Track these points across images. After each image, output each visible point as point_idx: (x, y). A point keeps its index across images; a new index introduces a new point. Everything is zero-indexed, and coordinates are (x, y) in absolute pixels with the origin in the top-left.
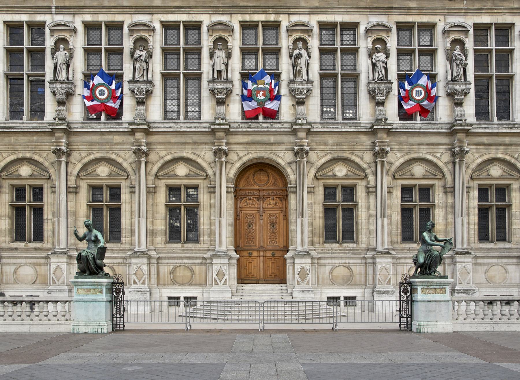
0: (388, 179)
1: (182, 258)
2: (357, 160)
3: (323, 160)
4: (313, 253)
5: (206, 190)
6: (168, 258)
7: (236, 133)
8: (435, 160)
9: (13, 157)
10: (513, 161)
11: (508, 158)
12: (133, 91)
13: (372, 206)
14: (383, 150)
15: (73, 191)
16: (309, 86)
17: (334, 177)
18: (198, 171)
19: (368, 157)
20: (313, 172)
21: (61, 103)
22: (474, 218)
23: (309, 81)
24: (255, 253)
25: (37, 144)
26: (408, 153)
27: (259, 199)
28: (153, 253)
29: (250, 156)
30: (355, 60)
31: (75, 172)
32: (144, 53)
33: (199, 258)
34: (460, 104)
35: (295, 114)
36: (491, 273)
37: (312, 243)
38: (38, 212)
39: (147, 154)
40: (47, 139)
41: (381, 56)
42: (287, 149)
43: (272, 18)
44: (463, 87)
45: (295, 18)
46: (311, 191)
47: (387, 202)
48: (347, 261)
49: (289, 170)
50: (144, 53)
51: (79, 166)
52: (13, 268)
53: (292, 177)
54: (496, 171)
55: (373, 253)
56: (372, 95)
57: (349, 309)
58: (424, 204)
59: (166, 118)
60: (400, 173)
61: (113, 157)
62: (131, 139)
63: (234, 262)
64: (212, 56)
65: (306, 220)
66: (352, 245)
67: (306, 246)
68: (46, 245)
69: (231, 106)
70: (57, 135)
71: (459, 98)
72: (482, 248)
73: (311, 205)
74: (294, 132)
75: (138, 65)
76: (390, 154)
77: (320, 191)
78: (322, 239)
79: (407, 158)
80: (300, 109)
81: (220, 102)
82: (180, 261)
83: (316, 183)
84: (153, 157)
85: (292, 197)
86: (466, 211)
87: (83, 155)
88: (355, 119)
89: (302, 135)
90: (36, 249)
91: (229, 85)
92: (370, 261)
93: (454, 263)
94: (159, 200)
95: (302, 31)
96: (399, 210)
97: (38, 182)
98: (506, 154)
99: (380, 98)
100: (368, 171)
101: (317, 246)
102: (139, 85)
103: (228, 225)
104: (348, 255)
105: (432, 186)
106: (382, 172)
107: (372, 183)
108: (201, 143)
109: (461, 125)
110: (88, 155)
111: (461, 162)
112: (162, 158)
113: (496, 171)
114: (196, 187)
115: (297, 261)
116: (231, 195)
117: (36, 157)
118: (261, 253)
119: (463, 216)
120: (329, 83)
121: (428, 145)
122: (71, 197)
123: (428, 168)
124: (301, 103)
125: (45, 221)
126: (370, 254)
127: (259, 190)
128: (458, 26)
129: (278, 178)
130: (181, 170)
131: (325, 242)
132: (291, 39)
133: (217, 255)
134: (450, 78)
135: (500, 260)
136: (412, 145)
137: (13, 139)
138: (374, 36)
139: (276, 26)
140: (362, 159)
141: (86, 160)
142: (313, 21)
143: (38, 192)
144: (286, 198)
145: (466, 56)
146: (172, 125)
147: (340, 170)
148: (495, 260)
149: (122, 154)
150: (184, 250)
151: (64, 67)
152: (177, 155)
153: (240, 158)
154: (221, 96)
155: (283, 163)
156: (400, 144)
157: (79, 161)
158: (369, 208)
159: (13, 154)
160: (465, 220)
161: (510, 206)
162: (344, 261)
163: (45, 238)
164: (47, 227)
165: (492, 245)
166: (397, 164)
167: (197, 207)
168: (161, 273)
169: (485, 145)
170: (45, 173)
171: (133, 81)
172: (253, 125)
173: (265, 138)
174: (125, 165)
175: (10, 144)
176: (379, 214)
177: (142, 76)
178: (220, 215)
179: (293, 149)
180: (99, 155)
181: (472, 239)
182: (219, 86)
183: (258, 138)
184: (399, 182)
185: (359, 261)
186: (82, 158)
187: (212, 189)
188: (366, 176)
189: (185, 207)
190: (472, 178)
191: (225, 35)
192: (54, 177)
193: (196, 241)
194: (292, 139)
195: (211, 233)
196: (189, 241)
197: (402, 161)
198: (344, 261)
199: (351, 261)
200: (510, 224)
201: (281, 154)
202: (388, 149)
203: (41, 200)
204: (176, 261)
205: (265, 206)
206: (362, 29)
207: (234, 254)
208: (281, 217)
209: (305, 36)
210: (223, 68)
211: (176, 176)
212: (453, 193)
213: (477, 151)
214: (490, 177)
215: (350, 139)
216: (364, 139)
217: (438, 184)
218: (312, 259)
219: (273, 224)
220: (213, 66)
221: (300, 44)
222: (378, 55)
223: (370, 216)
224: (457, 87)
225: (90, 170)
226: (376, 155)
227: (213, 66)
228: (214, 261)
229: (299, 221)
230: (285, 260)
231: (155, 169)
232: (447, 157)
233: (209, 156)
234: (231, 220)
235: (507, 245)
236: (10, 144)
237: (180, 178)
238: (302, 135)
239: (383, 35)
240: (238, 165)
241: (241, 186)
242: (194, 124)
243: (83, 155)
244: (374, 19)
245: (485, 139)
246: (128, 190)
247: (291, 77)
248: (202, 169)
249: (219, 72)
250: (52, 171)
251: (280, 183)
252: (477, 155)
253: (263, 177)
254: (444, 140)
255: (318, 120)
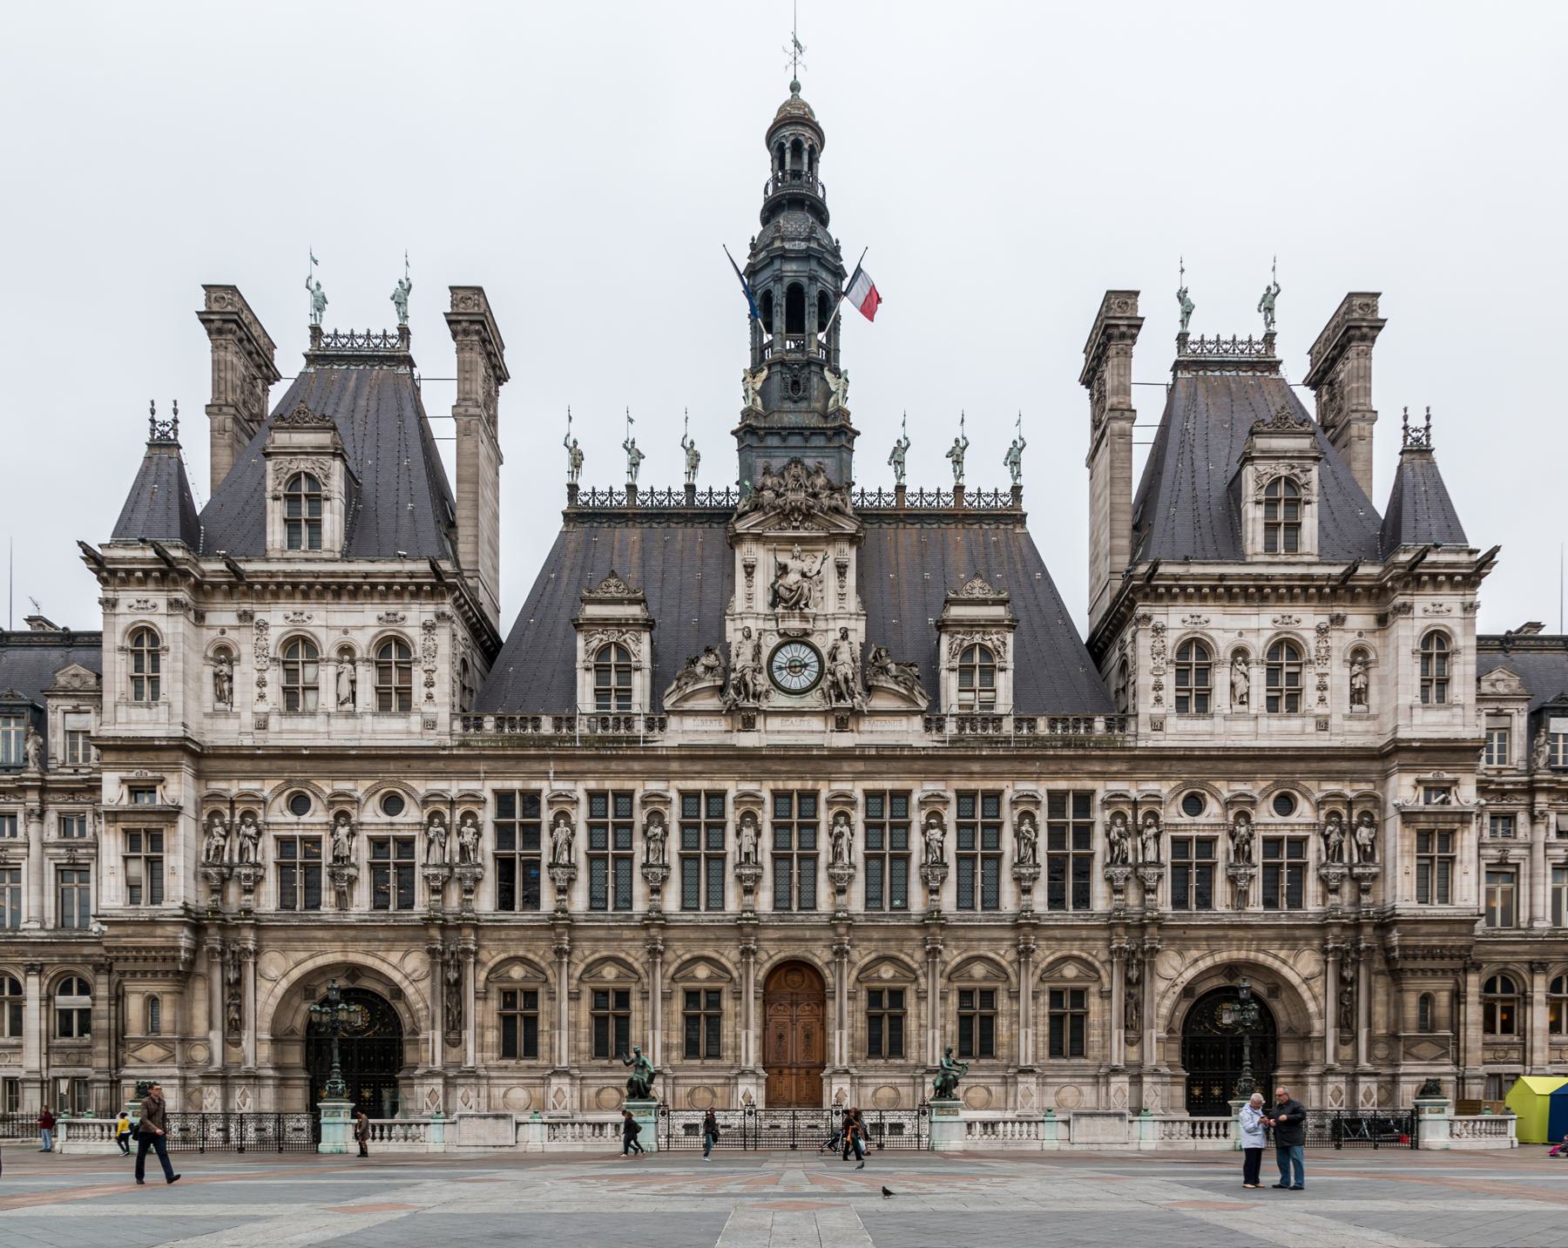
0: (940, 983)
1: (702, 1077)
2: (907, 959)
3: (867, 959)
4: (853, 1071)
5: (730, 995)
6: (686, 1077)
7: (766, 927)
8: (998, 958)
9: (503, 956)
10: (1090, 959)
11: (1084, 955)
12: (645, 877)
13: (923, 1015)
14: (935, 949)
15: (574, 997)
16: (851, 871)
17: (880, 979)
18: (721, 973)
19: (919, 955)
20: (855, 973)
21: (561, 891)
22: (1044, 1028)
23: (852, 866)
24: (786, 1071)
25: (532, 939)
26: (966, 951)
27: (791, 1005)
28: (668, 1071)
29: (782, 955)
30: (907, 835)
31: (577, 974)
32: (659, 830)
33: (722, 1077)
34: (1027, 891)
35: (834, 904)
36: (1063, 1095)
37: (852, 1059)
38: (531, 1022)
39: (662, 953)
40: (544, 934)
41: (936, 833)
42: (825, 946)
43: (809, 785)
44: (1031, 871)
45: (837, 786)
46: (852, 997)
47: (939, 1010)
48: (893, 1081)
49: (827, 972)
50: (659, 830)
51: (582, 966)
52: (502, 1090)
53: (830, 980)
54: (1070, 971)
55: (923, 1071)
56: (925, 881)
57: (895, 1138)
58: (985, 1011)
59: (683, 908)
60: (957, 974)
61: (622, 955)
62: (643, 934)
63: (763, 1081)
64: (738, 834)
65: (845, 1033)
66: (899, 1062)
67: (845, 1064)
68: (542, 1062)
69: (761, 894)
70: (558, 930)
71: (1027, 884)
72: (1053, 1065)
73: (852, 1014)
74: (833, 927)
75: (652, 846)
76: (945, 952)
77: (863, 996)
78: (866, 1053)
79: (965, 955)
80: (841, 899)
81: (748, 891)
82: (699, 1081)
83: (858, 986)
84: (669, 956)
85: (830, 1003)
86: (1031, 1020)
87: (587, 953)
88: (906, 908)
89: (842, 930)
90: (529, 1067)
91: (759, 871)
92: (919, 1080)
93: (1016, 1083)
94: (675, 1007)
95: (845, 803)
96: (955, 1018)
97: (531, 986)
98: (1082, 950)
99: (934, 884)
100: (919, 972)
101: (859, 1062)
102: (654, 870)
103: (756, 1037)
104: (894, 1073)
105: (996, 989)
106: (934, 975)
107: (923, 987)
108: (726, 940)
109: (1026, 918)
110: (593, 953)
111: (1027, 963)
112: (679, 957)
113: (1070, 971)
114: (718, 992)
115: (834, 1081)
116: (760, 1002)
117: (531, 956)
118: (794, 1071)
119: (1027, 1026)
120: (875, 863)
121: (990, 940)
122: (572, 1003)
123: (990, 968)
124: (841, 891)
125: (540, 1034)
126: (920, 1072)
127: (792, 994)
128: (1027, 796)
129: (815, 980)
130: (702, 972)
131: (868, 1057)
132: (832, 813)
133: (743, 1073)
134: (1016, 860)
135: (1073, 1080)
136: (971, 940)
137: (503, 934)
138: (929, 809)
139: (814, 795)
140: (912, 957)
141: (590, 959)
142: (857, 789)
143: (531, 997)
144: (823, 1003)
145: (1036, 832)
146: (692, 917)
147: (886, 971)
148: (1067, 1080)
149: (633, 952)
150: (704, 1068)
151: (566, 847)
152: (696, 953)
153: (770, 957)
154: (749, 884)
155: (820, 964)
156: (957, 939)
157: (582, 961)
158: (919, 1017)
159: (503, 951)
160: (1030, 1032)
161: (1087, 1013)
162: (889, 1081)
163: (540, 1054)
164: (543, 1040)
165: (1064, 1062)
166: (953, 963)
167: (719, 1017)
168: (677, 1096)
169: (1056, 939)
170: (541, 975)
171: (646, 865)
172: (786, 918)
173: (799, 933)
174: (636, 965)
175: (500, 940)
176: (930, 1026)
177: (658, 859)
178: (747, 1027)
179: (831, 947)
180: (605, 953)
181: (1041, 1053)
182: (747, 872)
183: (792, 933)
184: (956, 985)
185: (907, 1081)
186: (586, 957)
187: (737, 996)
188: (916, 978)
189: (705, 1015)
190: (1041, 979)
191: (754, 808)
192: (552, 980)
193: (718, 1056)
194: (831, 934)
195: (736, 1047)
196: (709, 1056)
197: (958, 959)
198: (889, 1081)
199: (898, 1081)
200: (1088, 1036)
201: (818, 953)
202: (941, 947)
203: (535, 1006)
204: (695, 1081)
205: (799, 1013)
206: (915, 799)
207: (762, 1072)
208: (817, 1026)
209: (847, 809)
210: (752, 849)
211: (695, 979)
212: (1018, 998)
213: (1048, 948)
214: (1063, 978)
215: (899, 933)
216: (915, 933)
217: (1000, 985)
218: (853, 1077)
219: (808, 1037)
220: (740, 846)
221: (842, 820)
222: (933, 832)
223: (920, 1026)
224: (1024, 871)
225: (594, 972)
226: (928, 953)
227: (740, 846)
228: (740, 1081)
229: (837, 1033)
230: (821, 1079)
231: (672, 970)
232: (1012, 955)
233: (734, 954)
234: (759, 1031)
235: (1083, 1061)
236: (500, 940)
237: (700, 981)
238: (842, 930)
239: (940, 808)
240: (767, 966)
241: (771, 988)
242: (716, 916)
243: (587, 953)
244: (931, 787)
245: (1057, 933)
246: (639, 995)
247: (831, 860)
248: (727, 971)
249: (747, 855)
250: (549, 972)
251: (817, 985)
252: (1047, 953)
253: (797, 978)
254: (1009, 934)
255: (862, 911)
